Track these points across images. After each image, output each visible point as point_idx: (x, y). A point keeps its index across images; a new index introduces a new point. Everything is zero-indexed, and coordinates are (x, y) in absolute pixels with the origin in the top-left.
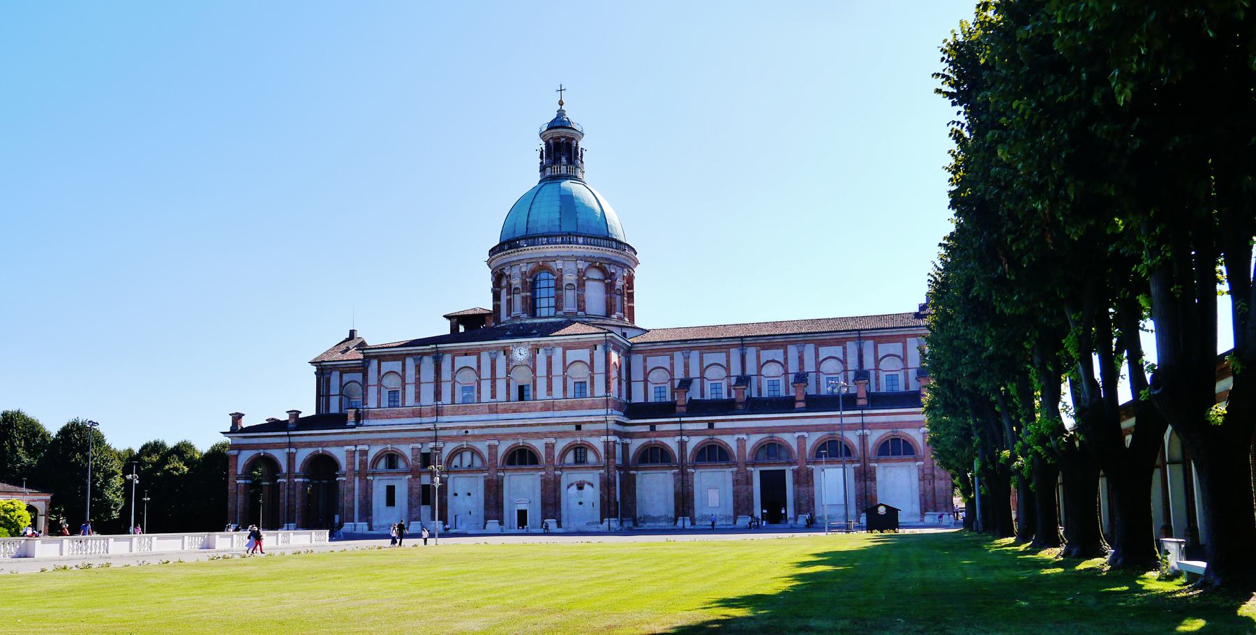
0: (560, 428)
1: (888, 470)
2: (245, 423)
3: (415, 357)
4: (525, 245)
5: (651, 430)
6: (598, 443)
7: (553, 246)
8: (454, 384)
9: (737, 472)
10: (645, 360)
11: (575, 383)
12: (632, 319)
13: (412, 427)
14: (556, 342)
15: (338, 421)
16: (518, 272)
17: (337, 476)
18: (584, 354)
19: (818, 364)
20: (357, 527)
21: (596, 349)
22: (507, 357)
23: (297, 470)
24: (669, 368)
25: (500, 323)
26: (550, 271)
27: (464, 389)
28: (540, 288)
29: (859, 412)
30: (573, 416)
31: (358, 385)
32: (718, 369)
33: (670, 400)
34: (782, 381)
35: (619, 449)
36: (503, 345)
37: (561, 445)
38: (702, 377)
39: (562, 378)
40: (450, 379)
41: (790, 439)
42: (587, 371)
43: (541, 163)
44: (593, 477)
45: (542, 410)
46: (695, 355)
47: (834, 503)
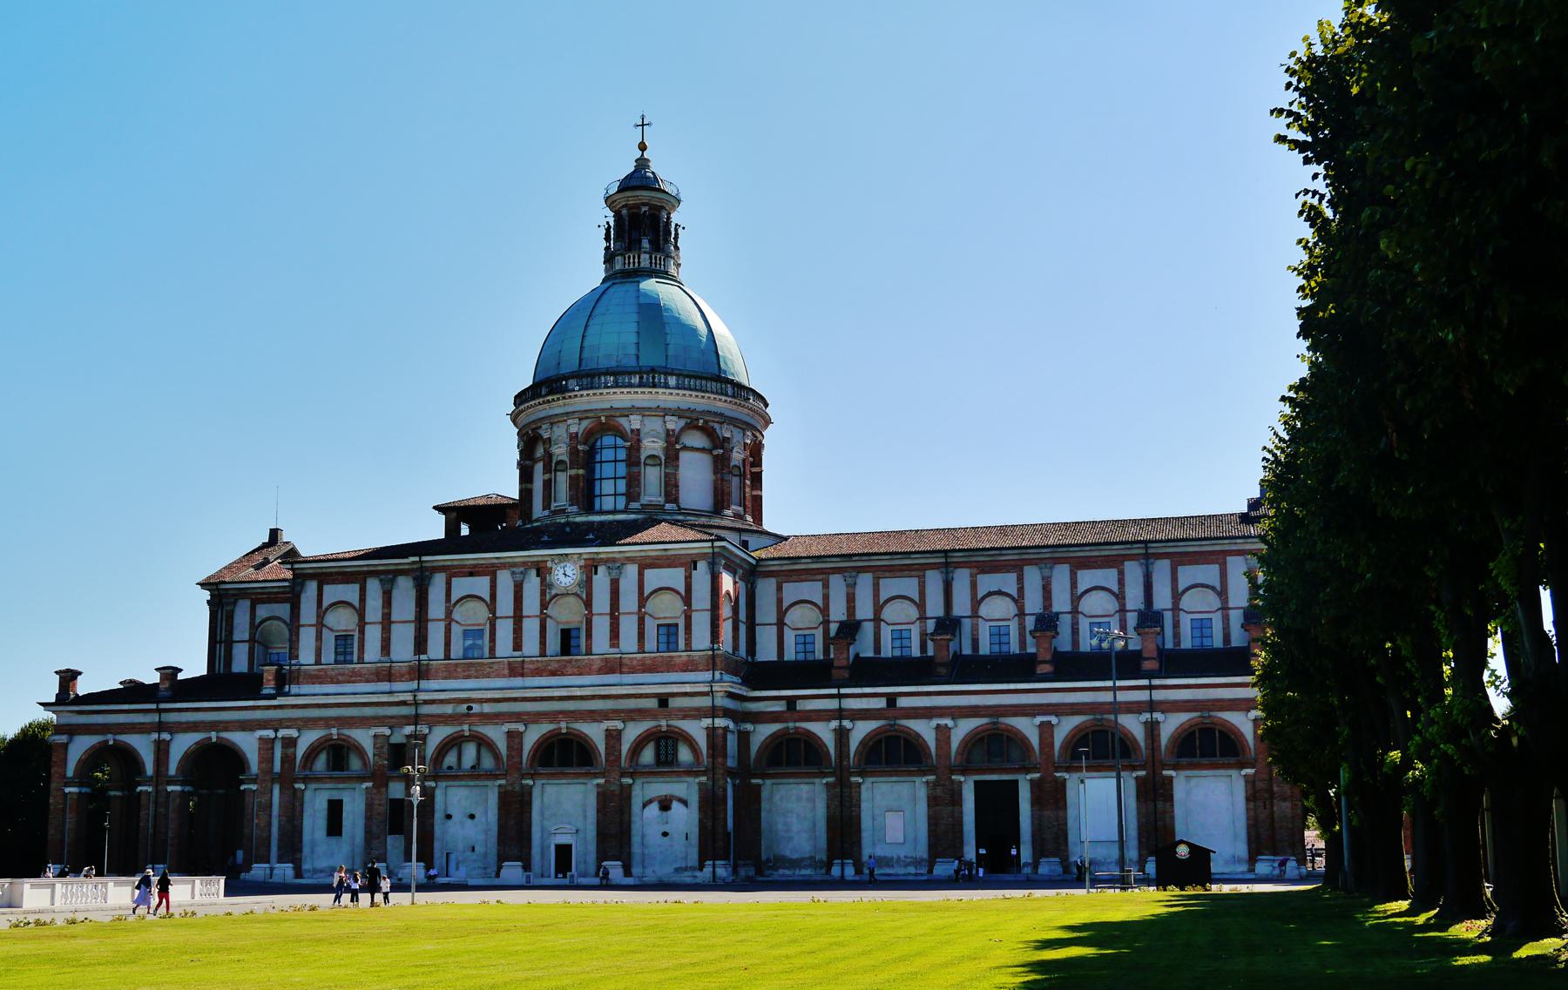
1: (1194, 782)
2: (83, 687)
3: (383, 577)
5: (788, 709)
6: (697, 729)
7: (625, 390)
8: (450, 624)
9: (936, 784)
10: (779, 589)
11: (659, 626)
12: (758, 518)
13: (374, 699)
15: (248, 686)
17: (242, 782)
18: (675, 577)
19: (1076, 599)
20: (275, 872)
21: (695, 569)
23: (172, 769)
24: (820, 604)
25: (531, 521)
26: (619, 432)
27: (466, 634)
28: (601, 462)
29: (1145, 682)
30: (655, 683)
33: (822, 657)
35: (732, 742)
36: (535, 559)
37: (632, 732)
38: (877, 619)
39: (635, 618)
41: (1028, 727)
42: (679, 606)
43: (607, 249)
44: (687, 788)
45: (601, 671)
47: (1103, 838)
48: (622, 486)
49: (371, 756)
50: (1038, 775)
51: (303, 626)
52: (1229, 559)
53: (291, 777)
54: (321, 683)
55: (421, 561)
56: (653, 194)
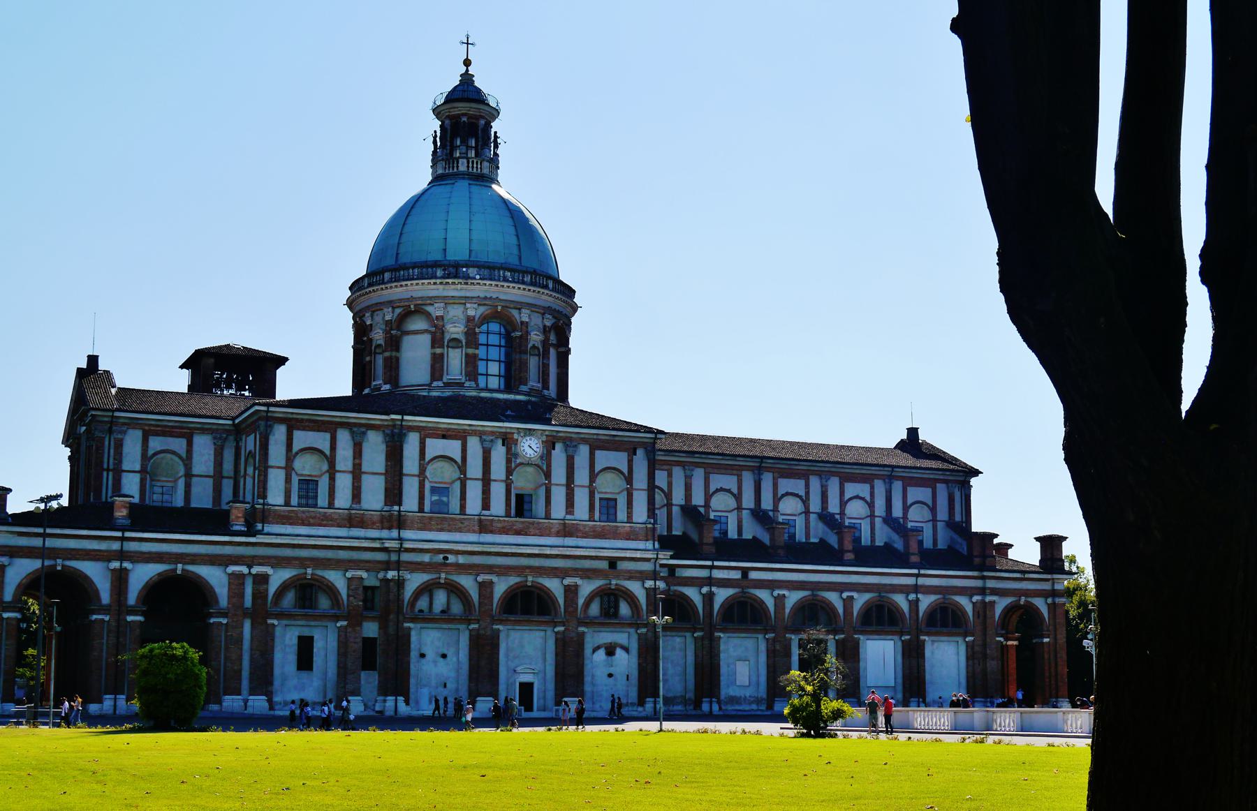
0: (587, 564)
1: (936, 644)
3: (355, 429)
4: (478, 277)
6: (636, 588)
7: (522, 287)
8: (424, 480)
11: (601, 499)
13: (356, 543)
14: (582, 436)
15: (214, 521)
16: (462, 317)
17: (211, 615)
18: (618, 459)
20: (250, 703)
21: (635, 454)
22: (509, 451)
23: (132, 598)
25: (399, 387)
29: (915, 571)
30: (611, 547)
31: (177, 459)
32: (726, 497)
34: (800, 523)
36: (503, 430)
37: (587, 588)
39: (587, 490)
40: (416, 472)
45: (558, 534)
46: (699, 474)
47: (880, 685)
48: (481, 368)
49: (344, 596)
50: (842, 636)
51: (272, 467)
52: (938, 485)
53: (262, 611)
54: (291, 524)
55: (402, 420)
56: (486, 108)
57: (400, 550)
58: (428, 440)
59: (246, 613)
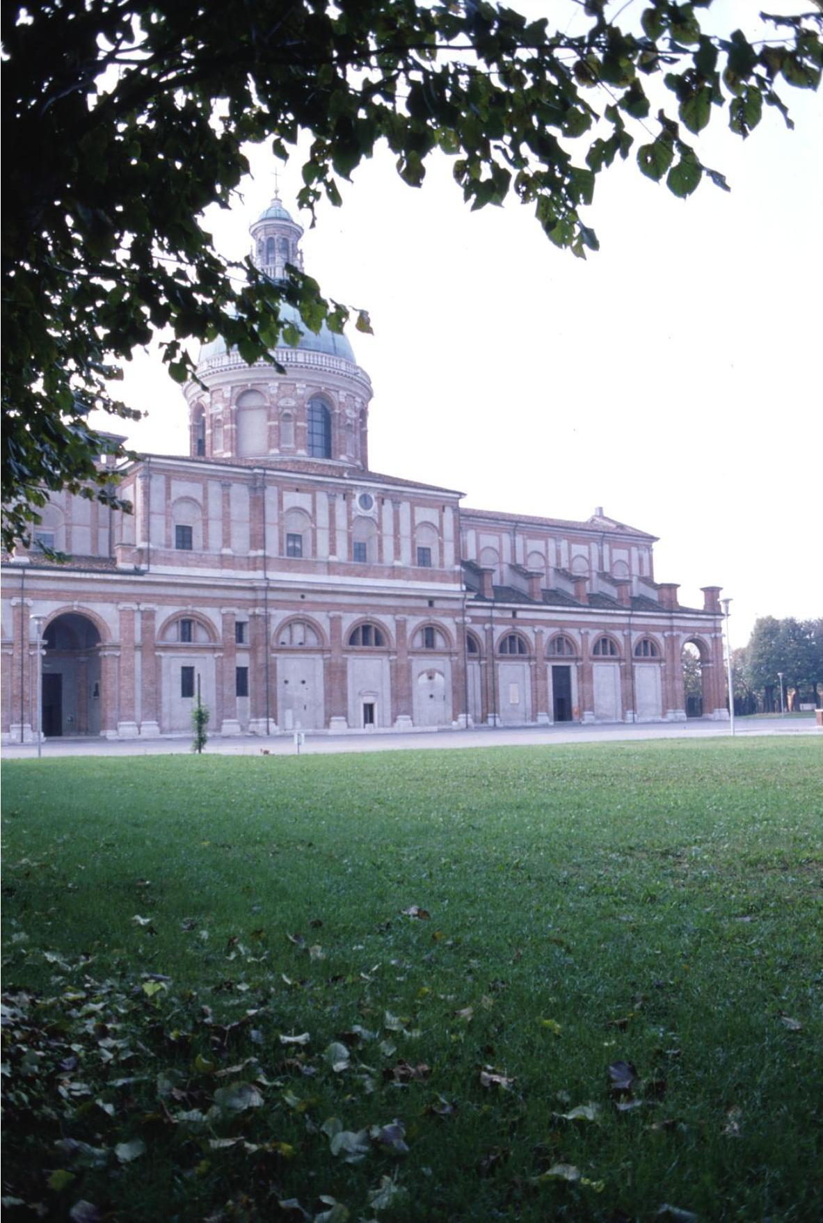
0: (412, 603)
6: (448, 623)
29: (629, 612)
55: (264, 475)
57: (267, 589)
58: (285, 493)
59: (136, 648)
